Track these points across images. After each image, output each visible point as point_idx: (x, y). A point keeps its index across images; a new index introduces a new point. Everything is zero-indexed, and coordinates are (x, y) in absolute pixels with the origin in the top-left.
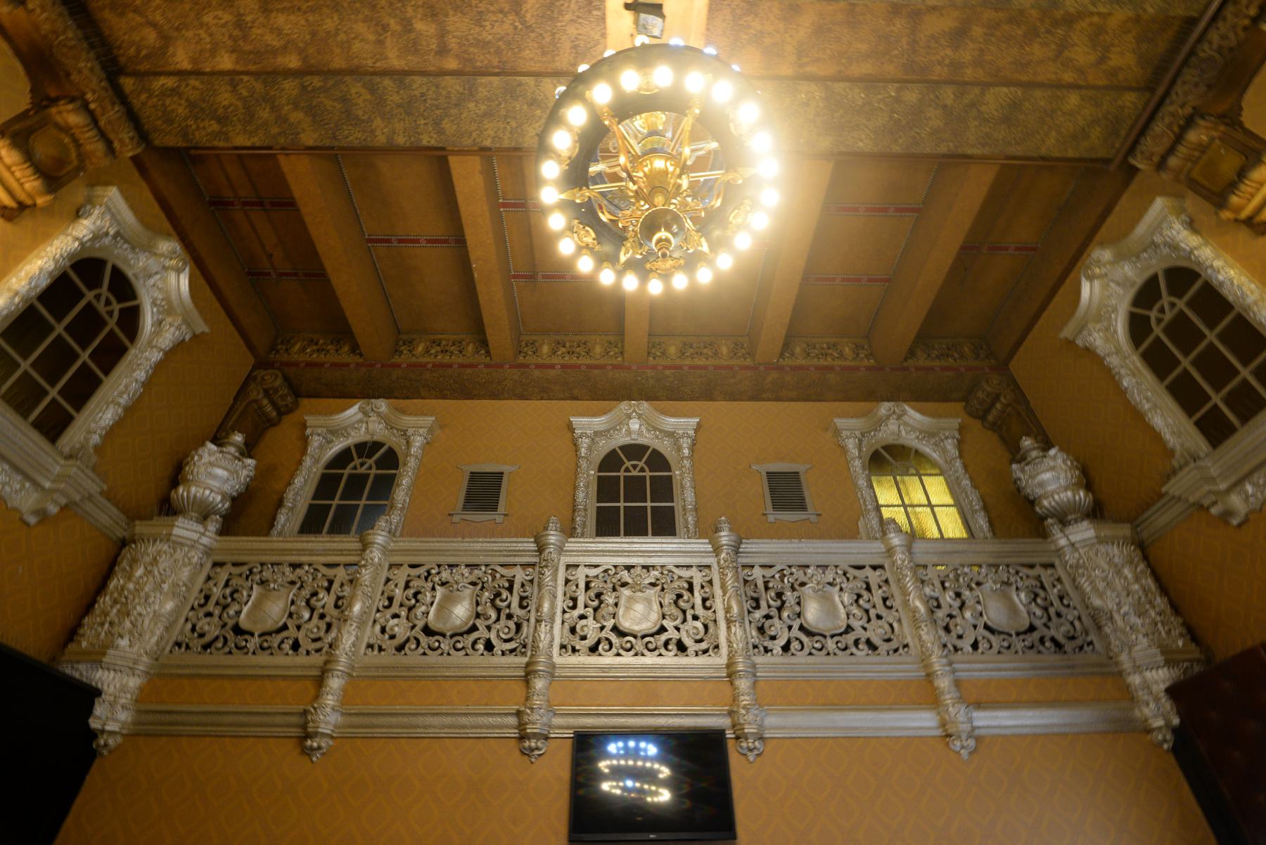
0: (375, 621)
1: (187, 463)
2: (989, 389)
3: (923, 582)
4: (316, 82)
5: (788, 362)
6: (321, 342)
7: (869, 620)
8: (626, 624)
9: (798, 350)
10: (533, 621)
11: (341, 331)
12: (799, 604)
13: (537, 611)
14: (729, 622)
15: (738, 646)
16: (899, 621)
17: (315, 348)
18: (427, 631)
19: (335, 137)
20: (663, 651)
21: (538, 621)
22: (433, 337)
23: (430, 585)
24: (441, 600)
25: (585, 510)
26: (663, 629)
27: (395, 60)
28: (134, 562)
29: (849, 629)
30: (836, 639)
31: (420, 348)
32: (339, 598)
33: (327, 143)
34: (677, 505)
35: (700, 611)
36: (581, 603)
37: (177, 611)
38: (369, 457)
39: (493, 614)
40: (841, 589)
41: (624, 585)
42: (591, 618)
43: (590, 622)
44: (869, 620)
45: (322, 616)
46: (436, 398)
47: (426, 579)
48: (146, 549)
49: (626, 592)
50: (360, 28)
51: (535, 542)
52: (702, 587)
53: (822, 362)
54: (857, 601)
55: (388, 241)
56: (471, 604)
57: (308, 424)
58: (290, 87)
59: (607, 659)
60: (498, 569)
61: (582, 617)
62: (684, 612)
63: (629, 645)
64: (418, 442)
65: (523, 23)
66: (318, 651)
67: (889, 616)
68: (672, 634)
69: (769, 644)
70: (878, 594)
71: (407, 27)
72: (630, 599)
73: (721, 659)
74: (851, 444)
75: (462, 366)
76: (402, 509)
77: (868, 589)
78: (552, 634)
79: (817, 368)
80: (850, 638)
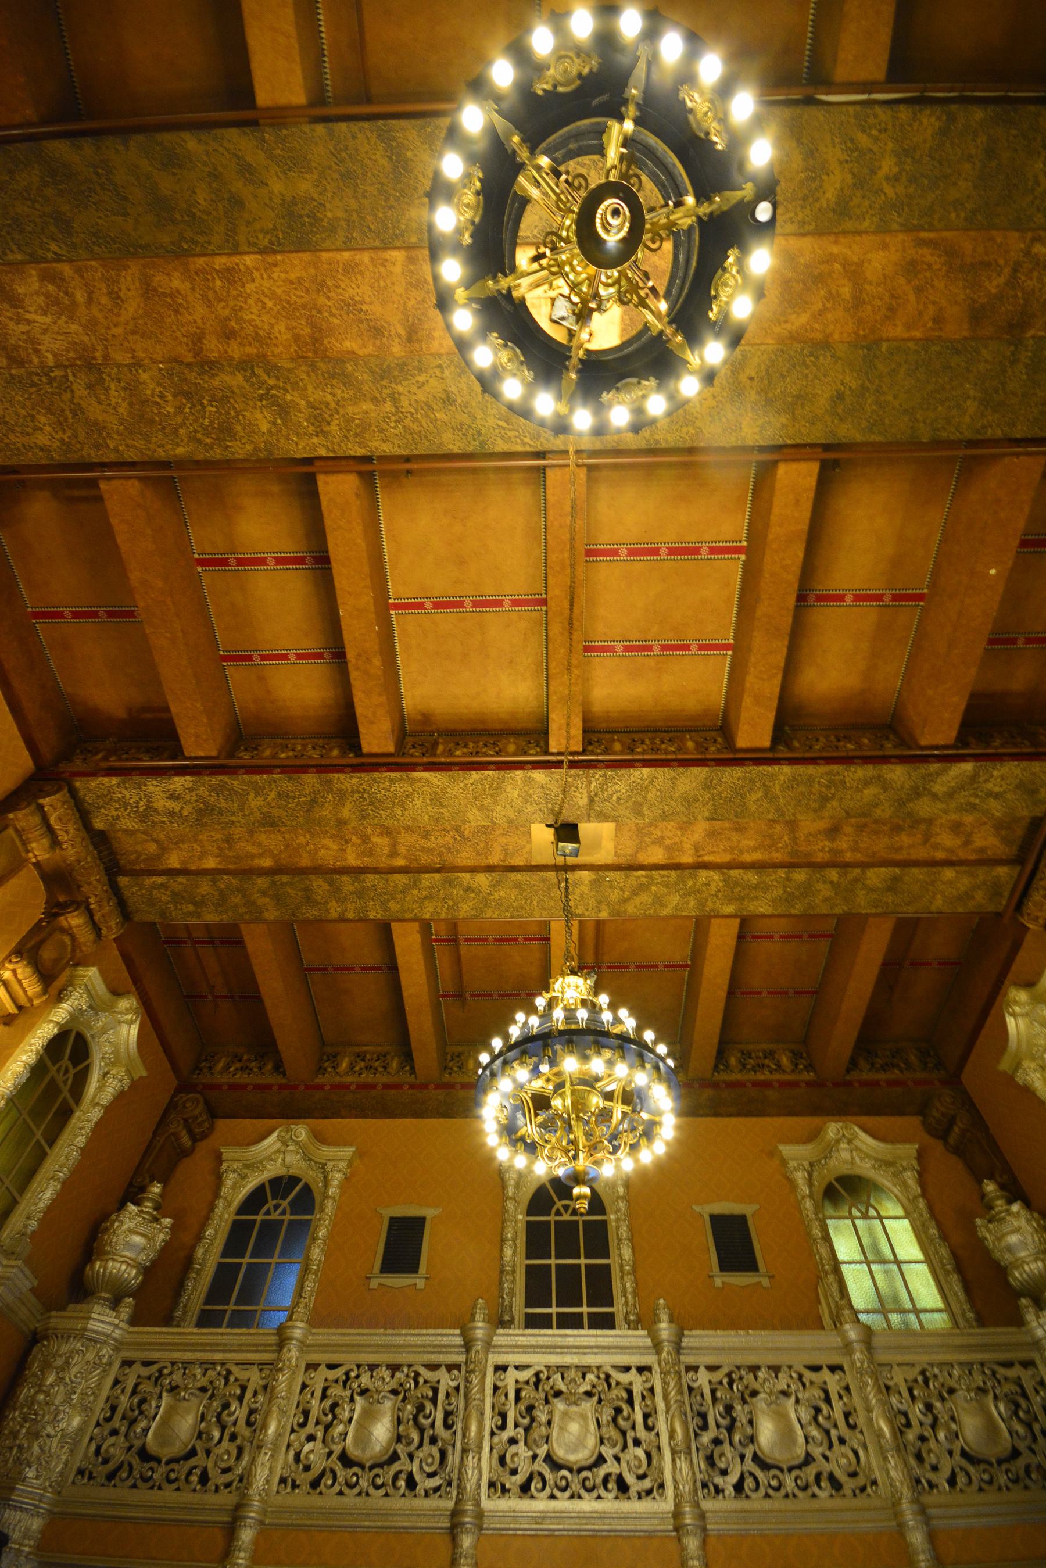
0: (289, 1446)
1: (107, 1229)
2: (943, 1109)
3: (888, 1388)
4: (285, 879)
5: (724, 1077)
6: (245, 1057)
7: (831, 1446)
8: (561, 1453)
9: (733, 1061)
10: (458, 1446)
11: (264, 1045)
12: (751, 1422)
13: (464, 1436)
14: (674, 1452)
15: (686, 1488)
16: (865, 1447)
17: (238, 1065)
18: (346, 1460)
19: (294, 914)
20: (602, 1492)
21: (465, 1451)
22: (357, 1049)
23: (348, 1393)
24: (360, 1417)
25: (514, 1271)
26: (601, 1460)
27: (352, 859)
28: (46, 1366)
29: (809, 1459)
30: (795, 1473)
31: (344, 1065)
32: (252, 1412)
34: (613, 1261)
35: (641, 1433)
36: (510, 1423)
37: (81, 1430)
38: (284, 1198)
39: (415, 1436)
40: (797, 1401)
41: (558, 1394)
42: (522, 1443)
43: (521, 1448)
44: (831, 1446)
45: (233, 1437)
46: (357, 1117)
47: (345, 1383)
48: (59, 1347)
49: (559, 1405)
51: (462, 1334)
52: (643, 1397)
53: (760, 1077)
54: (815, 1419)
55: (326, 969)
56: (392, 1421)
57: (224, 1157)
58: (262, 882)
59: (540, 1504)
60: (422, 1371)
61: (513, 1441)
62: (624, 1434)
63: (564, 1483)
64: (336, 1178)
66: (228, 1485)
67: (854, 1440)
68: (610, 1467)
69: (719, 1480)
70: (838, 1406)
72: (565, 1414)
73: (665, 1505)
74: (800, 1177)
75: (386, 1087)
76: (316, 1273)
77: (828, 1400)
78: (481, 1468)
79: (756, 1084)
80: (810, 1472)
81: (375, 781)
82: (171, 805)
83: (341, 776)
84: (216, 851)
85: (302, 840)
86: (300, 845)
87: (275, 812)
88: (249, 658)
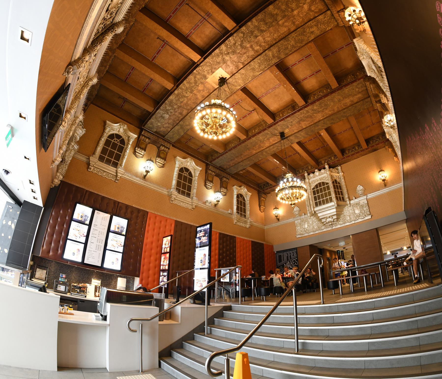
19: (265, 12)
33: (266, 10)
50: (269, 39)
65: (240, 62)
71: (260, 46)
82: (312, 30)
83: (276, 61)
84: (296, 17)
85: (276, 35)
86: (275, 33)
87: (286, 43)
88: (306, 58)
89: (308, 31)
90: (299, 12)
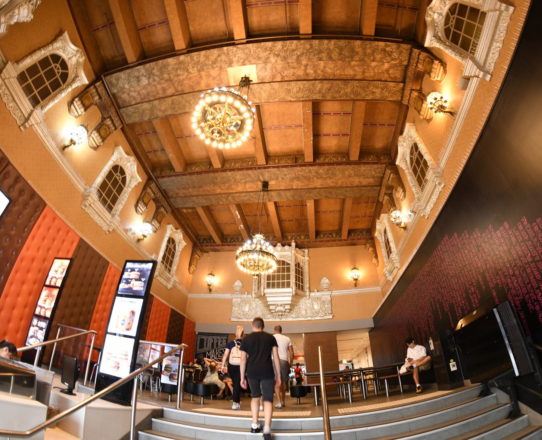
50: (329, 71)
81: (308, 97)
82: (375, 90)
83: (318, 98)
84: (370, 68)
87: (343, 86)
89: (371, 89)
90: (377, 66)
